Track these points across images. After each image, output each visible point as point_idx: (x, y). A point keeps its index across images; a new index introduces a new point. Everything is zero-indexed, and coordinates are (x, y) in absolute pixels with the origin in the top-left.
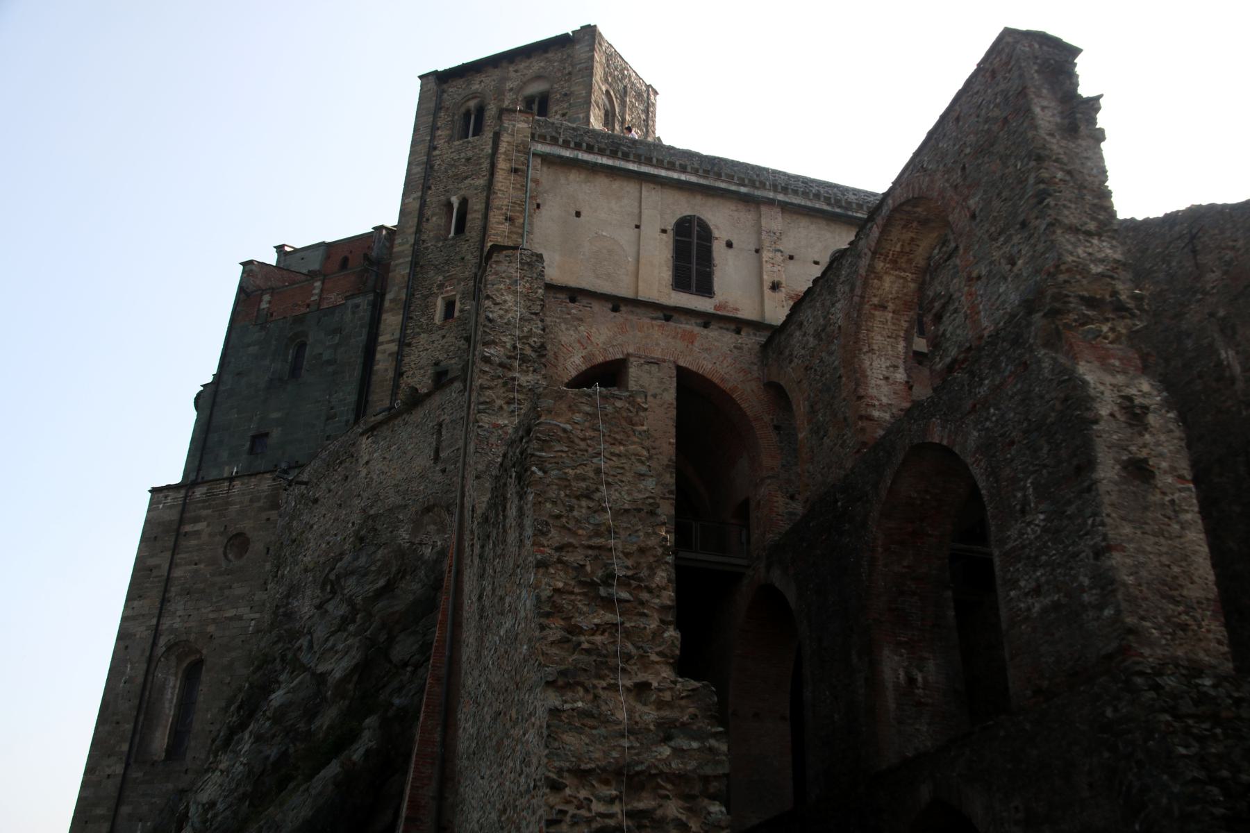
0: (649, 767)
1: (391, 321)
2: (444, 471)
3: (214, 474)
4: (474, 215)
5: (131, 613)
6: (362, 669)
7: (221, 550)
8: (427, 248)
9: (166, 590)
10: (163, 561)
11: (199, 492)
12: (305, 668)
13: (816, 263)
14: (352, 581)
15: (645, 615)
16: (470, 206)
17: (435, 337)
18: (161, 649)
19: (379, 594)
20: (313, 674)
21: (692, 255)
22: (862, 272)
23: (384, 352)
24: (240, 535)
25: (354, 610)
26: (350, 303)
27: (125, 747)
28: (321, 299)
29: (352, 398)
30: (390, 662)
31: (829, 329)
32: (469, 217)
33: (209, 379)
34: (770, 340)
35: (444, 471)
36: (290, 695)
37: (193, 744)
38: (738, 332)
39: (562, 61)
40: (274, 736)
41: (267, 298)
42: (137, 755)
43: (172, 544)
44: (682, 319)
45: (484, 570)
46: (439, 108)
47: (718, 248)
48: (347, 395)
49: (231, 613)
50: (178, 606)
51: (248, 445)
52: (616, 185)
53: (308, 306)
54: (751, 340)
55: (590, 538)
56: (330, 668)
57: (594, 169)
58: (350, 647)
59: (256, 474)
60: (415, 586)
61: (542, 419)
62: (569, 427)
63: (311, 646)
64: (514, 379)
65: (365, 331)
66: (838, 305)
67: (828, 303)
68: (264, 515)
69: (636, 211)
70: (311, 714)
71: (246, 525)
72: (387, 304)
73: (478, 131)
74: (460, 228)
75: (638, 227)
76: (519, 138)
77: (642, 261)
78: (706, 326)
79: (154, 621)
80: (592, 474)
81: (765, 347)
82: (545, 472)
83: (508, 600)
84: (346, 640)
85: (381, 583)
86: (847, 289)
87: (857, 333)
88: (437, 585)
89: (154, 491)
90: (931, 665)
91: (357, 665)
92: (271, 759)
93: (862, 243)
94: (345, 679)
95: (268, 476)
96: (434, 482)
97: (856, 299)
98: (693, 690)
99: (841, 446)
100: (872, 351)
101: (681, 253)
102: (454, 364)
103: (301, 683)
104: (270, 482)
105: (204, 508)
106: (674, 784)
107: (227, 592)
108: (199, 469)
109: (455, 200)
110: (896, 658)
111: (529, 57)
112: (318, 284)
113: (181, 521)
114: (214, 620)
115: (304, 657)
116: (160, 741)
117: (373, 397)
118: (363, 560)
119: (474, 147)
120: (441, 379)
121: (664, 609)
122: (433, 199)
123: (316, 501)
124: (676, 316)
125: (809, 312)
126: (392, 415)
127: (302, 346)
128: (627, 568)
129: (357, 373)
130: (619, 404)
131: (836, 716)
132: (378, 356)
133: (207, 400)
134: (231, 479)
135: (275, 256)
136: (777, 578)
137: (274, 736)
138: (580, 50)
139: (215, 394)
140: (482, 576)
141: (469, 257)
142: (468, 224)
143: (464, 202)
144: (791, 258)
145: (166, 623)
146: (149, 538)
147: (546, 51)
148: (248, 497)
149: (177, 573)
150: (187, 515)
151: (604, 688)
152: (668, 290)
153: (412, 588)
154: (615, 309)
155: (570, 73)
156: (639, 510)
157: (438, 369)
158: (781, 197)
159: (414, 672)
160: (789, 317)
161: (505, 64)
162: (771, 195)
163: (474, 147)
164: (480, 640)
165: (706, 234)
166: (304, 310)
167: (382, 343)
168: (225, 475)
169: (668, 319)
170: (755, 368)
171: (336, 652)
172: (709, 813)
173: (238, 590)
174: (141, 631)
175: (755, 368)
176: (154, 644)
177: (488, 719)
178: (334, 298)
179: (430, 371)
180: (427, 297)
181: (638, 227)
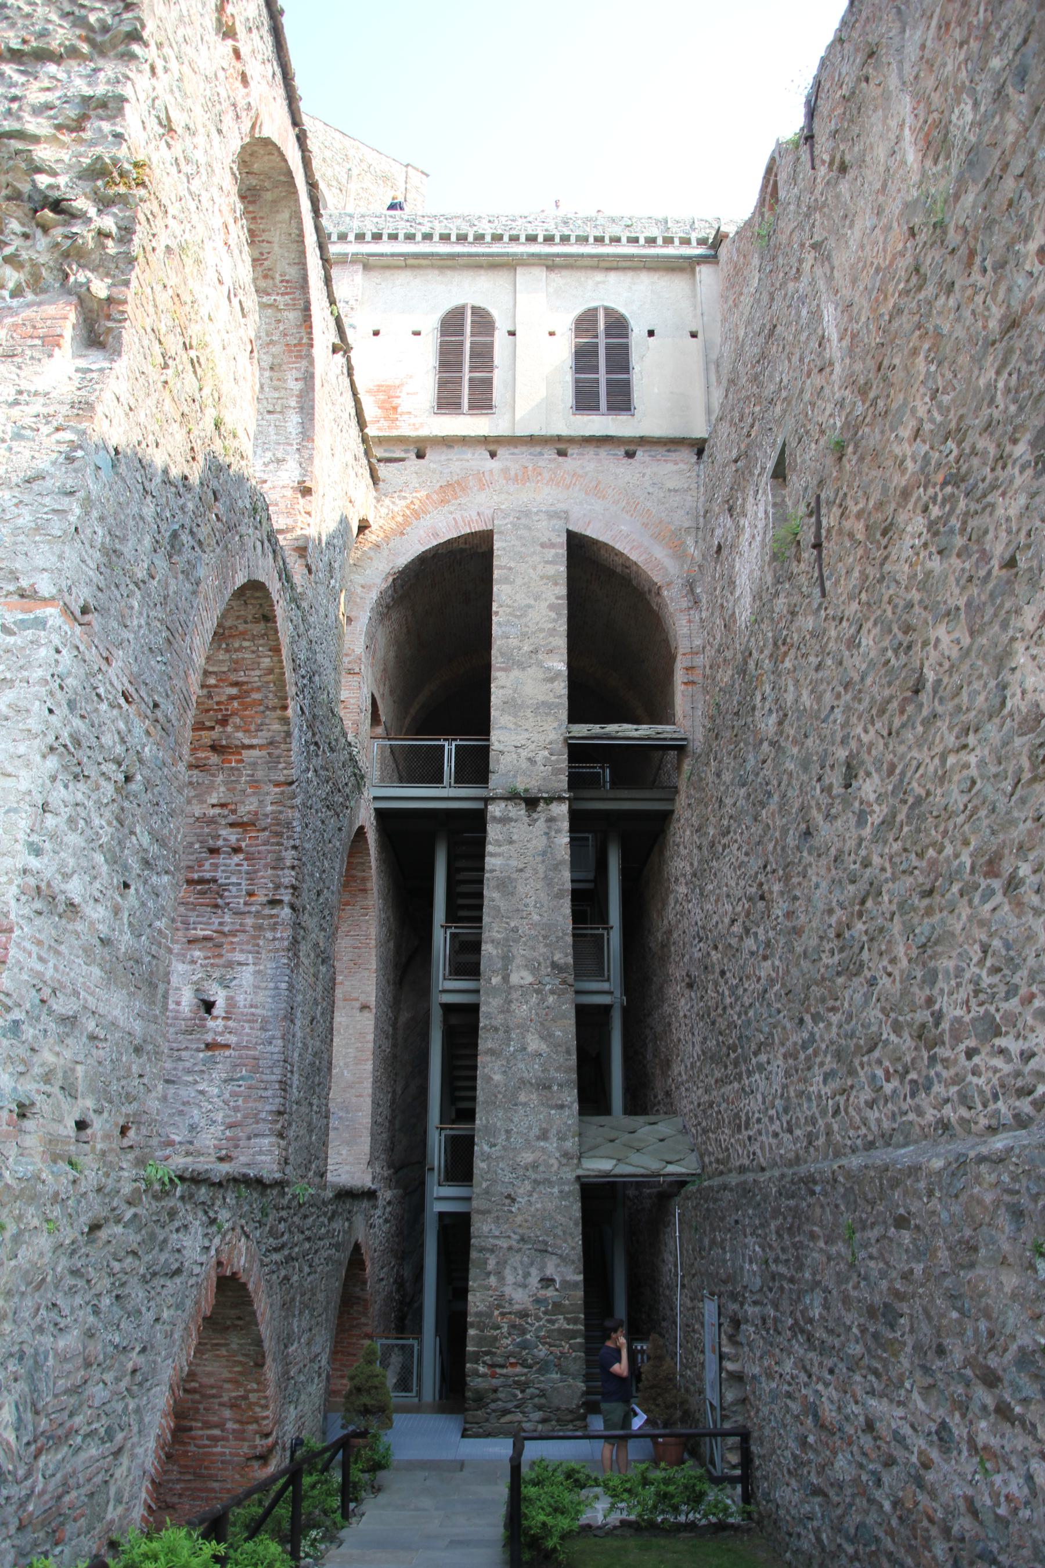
90: (246, 976)
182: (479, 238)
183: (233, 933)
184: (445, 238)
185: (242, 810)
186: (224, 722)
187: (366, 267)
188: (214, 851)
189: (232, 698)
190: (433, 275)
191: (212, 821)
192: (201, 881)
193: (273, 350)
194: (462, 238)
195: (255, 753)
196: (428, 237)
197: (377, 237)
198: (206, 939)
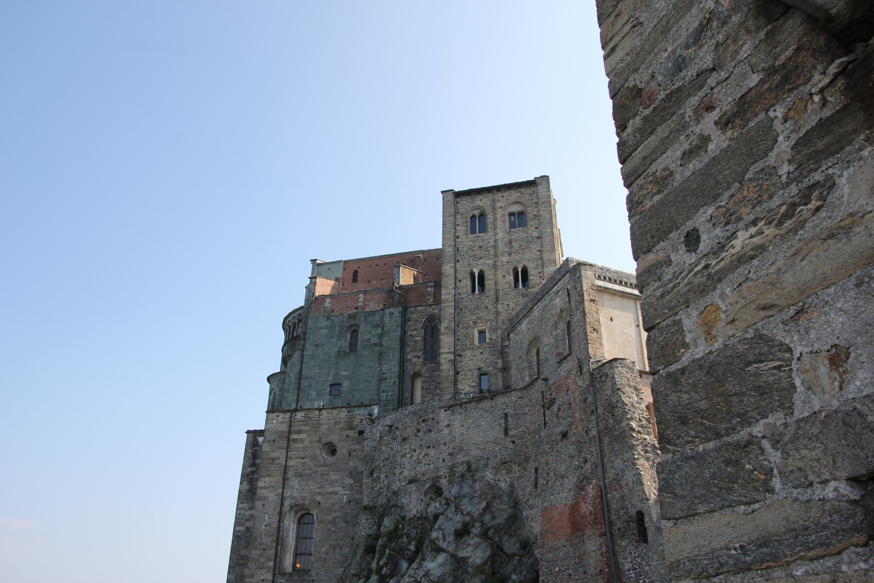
2: (514, 442)
3: (308, 405)
4: (490, 282)
6: (493, 556)
7: (318, 452)
8: (462, 298)
9: (285, 473)
11: (300, 415)
14: (465, 501)
16: (486, 276)
19: (485, 509)
23: (446, 358)
26: (387, 311)
27: (271, 564)
28: (365, 305)
29: (396, 369)
30: (504, 553)
32: (486, 282)
36: (442, 568)
41: (328, 300)
43: (286, 445)
46: (456, 212)
48: (391, 367)
49: (331, 490)
50: (294, 482)
51: (328, 389)
53: (356, 308)
56: (468, 555)
57: (615, 293)
58: (479, 544)
63: (444, 539)
64: (645, 439)
65: (399, 329)
68: (345, 433)
71: (333, 438)
73: (483, 229)
79: (280, 491)
84: (473, 538)
85: (484, 504)
94: (485, 563)
95: (344, 409)
103: (446, 560)
104: (346, 414)
105: (304, 425)
107: (326, 477)
108: (298, 401)
109: (476, 272)
111: (509, 189)
112: (361, 296)
113: (290, 432)
114: (320, 494)
115: (442, 544)
118: (466, 489)
119: (483, 240)
123: (404, 439)
129: (397, 354)
134: (320, 410)
135: (311, 266)
141: (490, 307)
142: (487, 287)
145: (288, 493)
149: (291, 463)
150: (293, 429)
155: (536, 203)
163: (483, 240)
167: (443, 353)
168: (316, 406)
171: (469, 545)
173: (333, 476)
176: (282, 505)
178: (372, 306)
179: (476, 373)
180: (466, 328)
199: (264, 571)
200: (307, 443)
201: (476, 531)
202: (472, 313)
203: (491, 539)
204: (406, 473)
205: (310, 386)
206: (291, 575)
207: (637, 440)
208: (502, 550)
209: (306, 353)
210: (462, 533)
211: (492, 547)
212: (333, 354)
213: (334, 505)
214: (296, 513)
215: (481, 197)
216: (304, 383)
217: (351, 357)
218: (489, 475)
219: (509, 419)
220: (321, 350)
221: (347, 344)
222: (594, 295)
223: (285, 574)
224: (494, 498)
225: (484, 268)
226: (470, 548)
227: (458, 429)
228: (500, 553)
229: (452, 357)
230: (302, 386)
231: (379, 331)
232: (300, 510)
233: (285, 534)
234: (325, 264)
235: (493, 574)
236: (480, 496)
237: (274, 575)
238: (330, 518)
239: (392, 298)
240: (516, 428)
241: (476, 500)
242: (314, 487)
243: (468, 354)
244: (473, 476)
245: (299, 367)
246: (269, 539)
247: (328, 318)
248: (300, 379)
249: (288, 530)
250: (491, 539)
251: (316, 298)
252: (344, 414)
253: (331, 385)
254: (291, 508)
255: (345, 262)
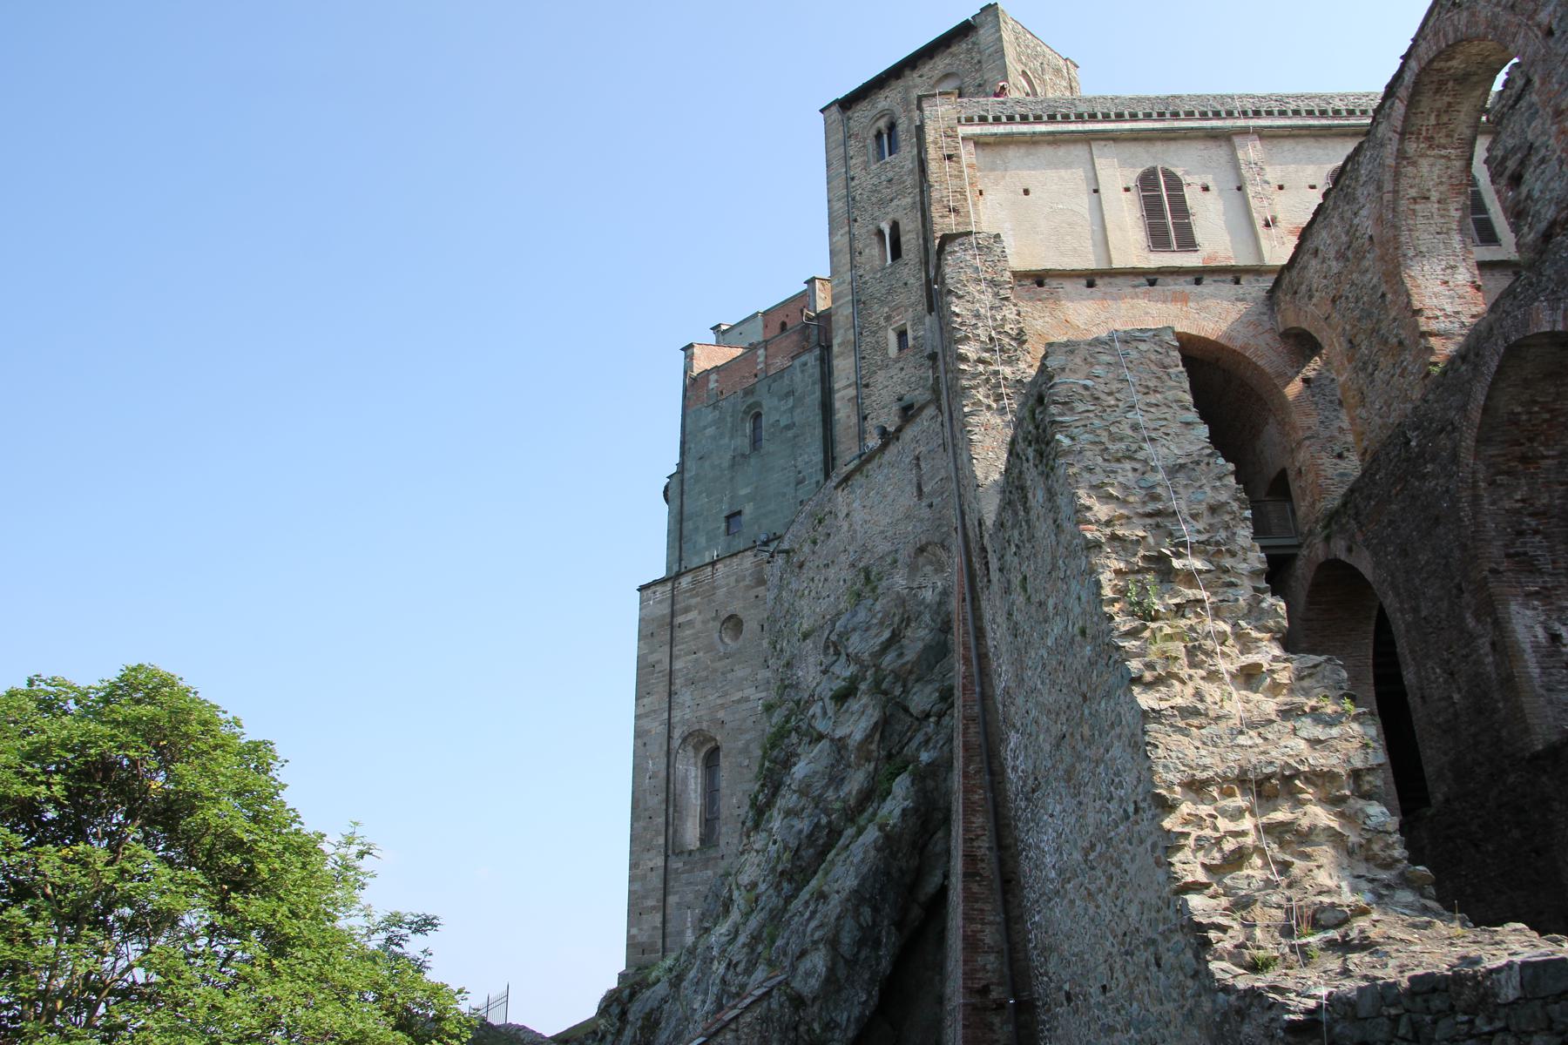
0: (1283, 768)
1: (843, 367)
2: (931, 506)
3: (696, 562)
5: (642, 711)
6: (883, 727)
7: (716, 635)
10: (662, 655)
11: (685, 582)
12: (821, 737)
13: (1313, 187)
14: (855, 638)
15: (1232, 585)
17: (893, 372)
18: (676, 742)
19: (886, 647)
20: (832, 740)
21: (1164, 211)
22: (1391, 161)
24: (731, 617)
25: (864, 667)
26: (797, 362)
27: (661, 840)
29: (819, 457)
31: (1355, 245)
32: (903, 239)
33: (674, 470)
34: (1277, 283)
35: (931, 506)
37: (724, 830)
38: (1237, 282)
39: (969, 51)
40: (803, 809)
41: (713, 377)
42: (672, 849)
44: (1169, 280)
45: (1009, 582)
46: (848, 137)
47: (1192, 196)
50: (685, 697)
51: (723, 525)
52: (1062, 151)
54: (1257, 288)
55: (1144, 503)
56: (848, 731)
57: (1033, 141)
58: (866, 706)
59: (735, 554)
60: (922, 633)
61: (1056, 380)
62: (1089, 383)
63: (825, 713)
64: (996, 373)
65: (818, 387)
66: (1363, 212)
67: (1349, 214)
69: (1091, 175)
70: (836, 780)
71: (735, 607)
72: (835, 349)
74: (896, 253)
75: (1096, 191)
76: (942, 125)
77: (1109, 226)
78: (1198, 282)
79: (666, 715)
80: (1129, 432)
81: (1271, 293)
82: (1073, 439)
83: (1051, 602)
85: (886, 634)
86: (1372, 189)
87: (1396, 237)
88: (946, 628)
89: (642, 589)
91: (876, 724)
92: (805, 833)
93: (1381, 128)
94: (868, 739)
96: (921, 520)
97: (1388, 197)
98: (1315, 666)
99: (1402, 375)
100: (1420, 254)
101: (1152, 208)
102: (920, 395)
104: (752, 559)
106: (1315, 785)
107: (729, 676)
108: (681, 560)
110: (1528, 613)
112: (761, 352)
113: (673, 615)
115: (821, 725)
116: (691, 833)
117: (840, 448)
118: (862, 615)
120: (908, 412)
121: (1254, 574)
122: (862, 230)
124: (1161, 279)
125: (1324, 234)
126: (866, 459)
127: (758, 416)
128: (1199, 532)
129: (819, 431)
130: (1143, 347)
131: (1456, 697)
132: (837, 405)
133: (676, 491)
134: (713, 563)
136: (1339, 549)
137: (803, 809)
138: (984, 35)
139: (682, 482)
140: (1007, 591)
141: (912, 281)
142: (904, 247)
143: (895, 227)
144: (1281, 188)
145: (677, 715)
146: (646, 635)
147: (949, 47)
148: (733, 579)
149: (678, 665)
150: (677, 607)
151: (1203, 678)
152: (1146, 253)
153: (918, 637)
154: (1091, 285)
156: (1198, 463)
157: (903, 404)
158: (1253, 122)
159: (938, 723)
160: (1298, 248)
161: (907, 72)
162: (1241, 123)
164: (1019, 664)
165: (1175, 184)
166: (753, 380)
169: (1152, 283)
170: (1265, 318)
172: (1368, 817)
173: (740, 672)
174: (656, 727)
175: (1265, 318)
176: (670, 737)
177: (1047, 748)
178: (780, 362)
179: (895, 408)
180: (875, 333)
181: (1096, 191)
182: (1337, 113)
183: (1555, 588)
184: (1310, 113)
185: (1538, 504)
186: (1531, 440)
187: (1261, 137)
188: (1520, 533)
189: (1545, 421)
190: (1311, 142)
191: (1518, 512)
192: (1517, 554)
193: (1442, 188)
194: (1323, 113)
195: (1550, 462)
196: (1296, 113)
197: (1257, 113)
198: (1537, 593)
199: (654, 852)
200: (698, 625)
201: (863, 686)
202: (882, 302)
203: (885, 693)
204: (805, 626)
205: (696, 529)
206: (690, 853)
207: (975, 376)
208: (906, 710)
209: (687, 475)
210: (842, 697)
211: (884, 707)
212: (726, 464)
213: (744, 720)
214: (696, 749)
215: (886, 92)
216: (689, 525)
217: (753, 461)
218: (900, 581)
219: (923, 465)
220: (707, 464)
221: (747, 441)
222: (967, 154)
223: (682, 852)
224: (906, 621)
225: (898, 216)
226: (855, 717)
227: (858, 516)
228: (901, 715)
229: (852, 392)
230: (685, 533)
231: (791, 401)
232: (702, 744)
233: (679, 787)
234: (732, 328)
235: (890, 756)
236: (881, 623)
237: (667, 857)
238: (740, 744)
239: (807, 339)
240: (931, 478)
241: (873, 632)
242: (713, 698)
243: (881, 376)
244: (873, 590)
245: (678, 502)
246: (656, 799)
247: (715, 406)
248: (681, 521)
249: (686, 778)
250: (885, 693)
251: (694, 380)
252: (748, 562)
253: (728, 518)
254: (684, 740)
255: (764, 313)
